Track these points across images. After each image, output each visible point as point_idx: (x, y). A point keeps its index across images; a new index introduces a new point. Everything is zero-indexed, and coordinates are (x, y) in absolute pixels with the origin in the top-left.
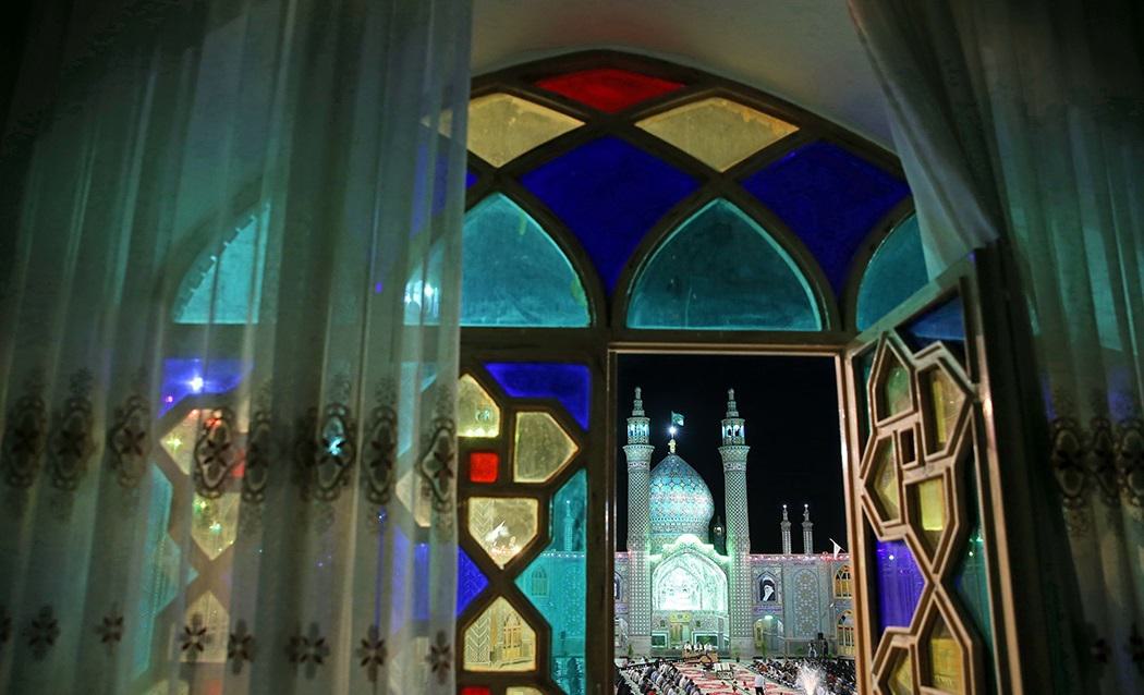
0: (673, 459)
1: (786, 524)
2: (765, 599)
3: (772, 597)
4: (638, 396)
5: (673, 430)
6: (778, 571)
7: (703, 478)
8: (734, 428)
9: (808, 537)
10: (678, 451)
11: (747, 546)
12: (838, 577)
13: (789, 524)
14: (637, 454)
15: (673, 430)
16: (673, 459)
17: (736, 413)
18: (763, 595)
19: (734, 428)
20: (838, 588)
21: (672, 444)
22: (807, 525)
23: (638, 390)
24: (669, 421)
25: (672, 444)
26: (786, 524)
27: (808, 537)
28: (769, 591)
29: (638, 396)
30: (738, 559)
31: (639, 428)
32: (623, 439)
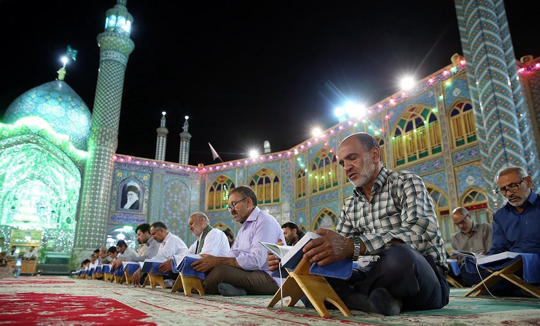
1: (163, 130)
2: (128, 206)
3: (136, 206)
5: (65, 60)
6: (146, 178)
7: (80, 96)
9: (184, 147)
10: (67, 79)
11: (113, 145)
12: (212, 190)
13: (166, 131)
18: (124, 201)
21: (62, 73)
25: (62, 73)
26: (163, 130)
27: (184, 147)
28: (132, 198)
30: (98, 156)
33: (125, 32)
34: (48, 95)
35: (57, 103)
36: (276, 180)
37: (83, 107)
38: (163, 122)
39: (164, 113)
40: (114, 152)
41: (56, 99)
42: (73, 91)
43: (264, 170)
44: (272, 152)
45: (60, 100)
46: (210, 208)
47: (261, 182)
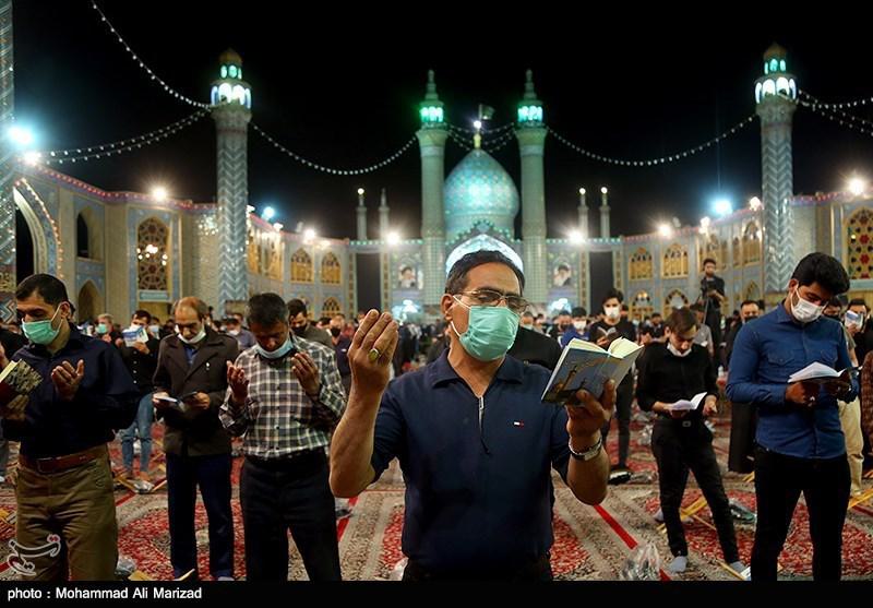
0: (478, 153)
4: (431, 78)
5: (477, 124)
8: (530, 113)
10: (483, 147)
12: (633, 260)
14: (430, 148)
15: (477, 124)
16: (478, 153)
17: (531, 95)
19: (530, 113)
20: (633, 269)
21: (477, 139)
22: (605, 207)
23: (431, 73)
24: (476, 117)
25: (477, 139)
29: (431, 78)
31: (432, 113)
32: (416, 124)
33: (536, 121)
34: (474, 174)
35: (482, 182)
36: (685, 254)
37: (505, 177)
38: (583, 201)
39: (582, 191)
40: (544, 237)
41: (480, 177)
42: (493, 161)
43: (676, 244)
44: (682, 227)
45: (485, 177)
46: (633, 277)
47: (673, 255)
